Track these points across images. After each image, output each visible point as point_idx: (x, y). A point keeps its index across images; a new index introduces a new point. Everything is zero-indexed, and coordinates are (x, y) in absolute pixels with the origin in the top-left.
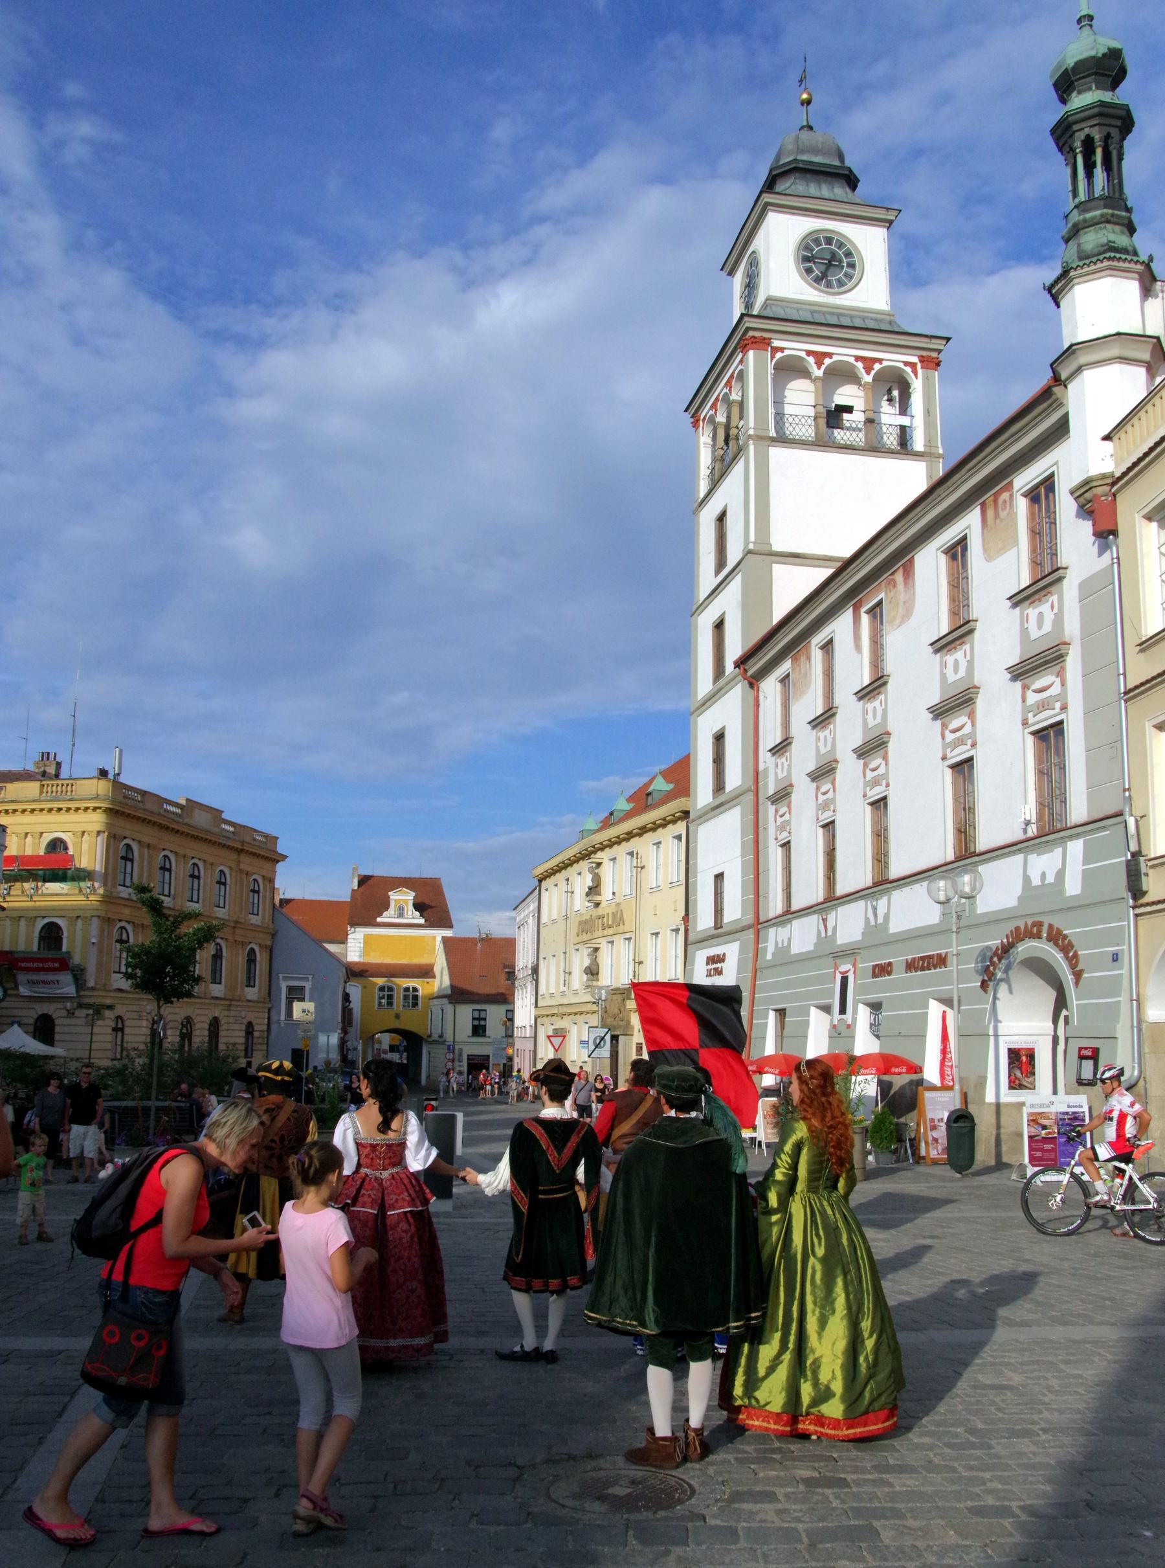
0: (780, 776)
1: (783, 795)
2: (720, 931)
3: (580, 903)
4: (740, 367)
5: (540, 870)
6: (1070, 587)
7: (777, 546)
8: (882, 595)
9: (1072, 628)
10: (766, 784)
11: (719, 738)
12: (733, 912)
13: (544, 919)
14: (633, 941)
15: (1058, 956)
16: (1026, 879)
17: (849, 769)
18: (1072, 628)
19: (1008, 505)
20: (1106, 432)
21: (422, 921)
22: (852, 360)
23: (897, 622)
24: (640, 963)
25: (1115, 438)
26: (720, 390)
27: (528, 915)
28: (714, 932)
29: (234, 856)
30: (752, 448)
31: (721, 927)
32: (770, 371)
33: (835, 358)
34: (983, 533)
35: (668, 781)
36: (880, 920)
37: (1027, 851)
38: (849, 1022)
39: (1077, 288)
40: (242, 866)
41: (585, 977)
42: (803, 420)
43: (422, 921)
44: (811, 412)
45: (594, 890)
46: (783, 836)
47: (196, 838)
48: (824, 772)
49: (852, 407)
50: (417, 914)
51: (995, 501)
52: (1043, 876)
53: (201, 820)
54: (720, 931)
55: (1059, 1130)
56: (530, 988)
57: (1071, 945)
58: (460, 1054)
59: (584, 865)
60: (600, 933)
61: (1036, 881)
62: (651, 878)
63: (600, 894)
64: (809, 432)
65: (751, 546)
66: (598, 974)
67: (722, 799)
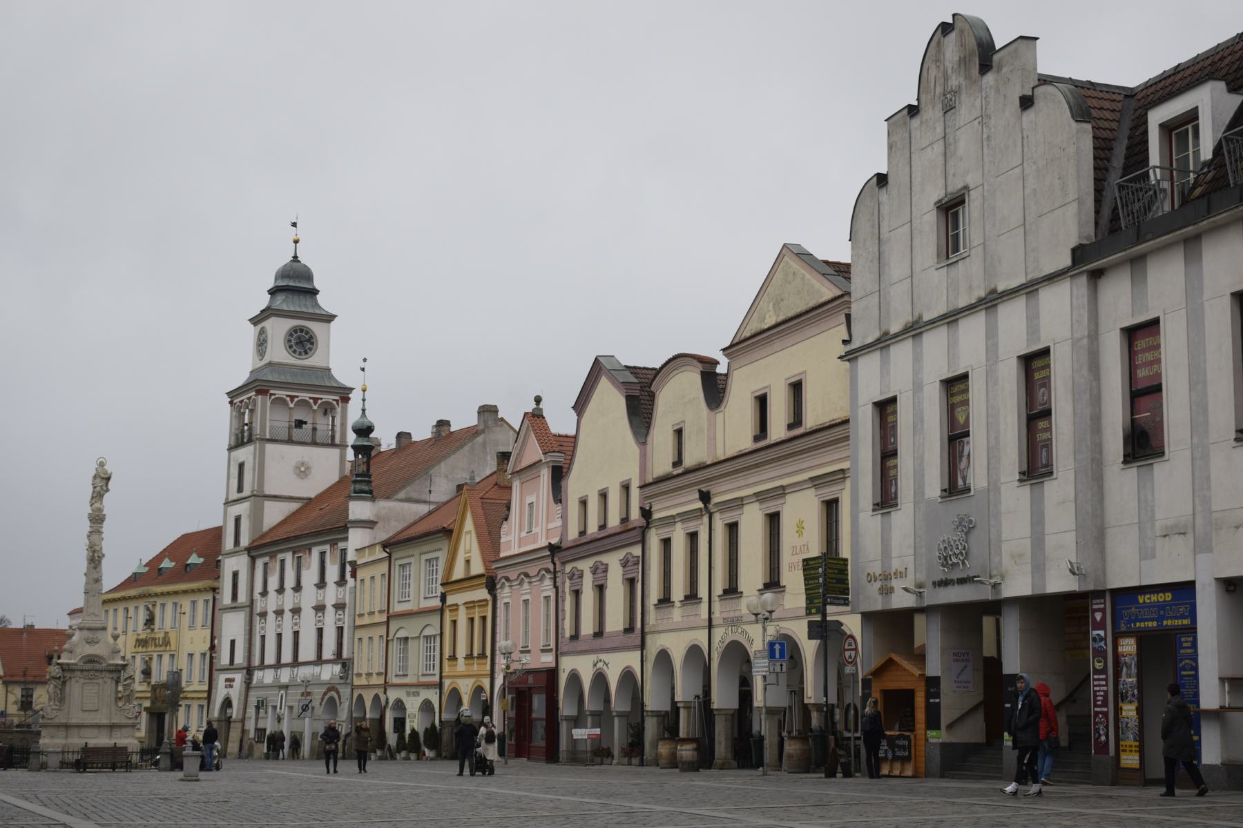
0: (263, 606)
1: (263, 615)
2: (232, 666)
7: (267, 492)
10: (257, 607)
12: (240, 659)
14: (176, 656)
16: (332, 673)
17: (288, 615)
18: (347, 601)
22: (308, 399)
26: (244, 397)
28: (228, 667)
33: (300, 398)
35: (200, 556)
37: (333, 663)
41: (142, 676)
44: (287, 425)
45: (150, 621)
46: (262, 632)
48: (279, 613)
54: (232, 666)
59: (142, 605)
60: (153, 648)
61: (334, 674)
63: (154, 625)
65: (255, 492)
67: (234, 605)
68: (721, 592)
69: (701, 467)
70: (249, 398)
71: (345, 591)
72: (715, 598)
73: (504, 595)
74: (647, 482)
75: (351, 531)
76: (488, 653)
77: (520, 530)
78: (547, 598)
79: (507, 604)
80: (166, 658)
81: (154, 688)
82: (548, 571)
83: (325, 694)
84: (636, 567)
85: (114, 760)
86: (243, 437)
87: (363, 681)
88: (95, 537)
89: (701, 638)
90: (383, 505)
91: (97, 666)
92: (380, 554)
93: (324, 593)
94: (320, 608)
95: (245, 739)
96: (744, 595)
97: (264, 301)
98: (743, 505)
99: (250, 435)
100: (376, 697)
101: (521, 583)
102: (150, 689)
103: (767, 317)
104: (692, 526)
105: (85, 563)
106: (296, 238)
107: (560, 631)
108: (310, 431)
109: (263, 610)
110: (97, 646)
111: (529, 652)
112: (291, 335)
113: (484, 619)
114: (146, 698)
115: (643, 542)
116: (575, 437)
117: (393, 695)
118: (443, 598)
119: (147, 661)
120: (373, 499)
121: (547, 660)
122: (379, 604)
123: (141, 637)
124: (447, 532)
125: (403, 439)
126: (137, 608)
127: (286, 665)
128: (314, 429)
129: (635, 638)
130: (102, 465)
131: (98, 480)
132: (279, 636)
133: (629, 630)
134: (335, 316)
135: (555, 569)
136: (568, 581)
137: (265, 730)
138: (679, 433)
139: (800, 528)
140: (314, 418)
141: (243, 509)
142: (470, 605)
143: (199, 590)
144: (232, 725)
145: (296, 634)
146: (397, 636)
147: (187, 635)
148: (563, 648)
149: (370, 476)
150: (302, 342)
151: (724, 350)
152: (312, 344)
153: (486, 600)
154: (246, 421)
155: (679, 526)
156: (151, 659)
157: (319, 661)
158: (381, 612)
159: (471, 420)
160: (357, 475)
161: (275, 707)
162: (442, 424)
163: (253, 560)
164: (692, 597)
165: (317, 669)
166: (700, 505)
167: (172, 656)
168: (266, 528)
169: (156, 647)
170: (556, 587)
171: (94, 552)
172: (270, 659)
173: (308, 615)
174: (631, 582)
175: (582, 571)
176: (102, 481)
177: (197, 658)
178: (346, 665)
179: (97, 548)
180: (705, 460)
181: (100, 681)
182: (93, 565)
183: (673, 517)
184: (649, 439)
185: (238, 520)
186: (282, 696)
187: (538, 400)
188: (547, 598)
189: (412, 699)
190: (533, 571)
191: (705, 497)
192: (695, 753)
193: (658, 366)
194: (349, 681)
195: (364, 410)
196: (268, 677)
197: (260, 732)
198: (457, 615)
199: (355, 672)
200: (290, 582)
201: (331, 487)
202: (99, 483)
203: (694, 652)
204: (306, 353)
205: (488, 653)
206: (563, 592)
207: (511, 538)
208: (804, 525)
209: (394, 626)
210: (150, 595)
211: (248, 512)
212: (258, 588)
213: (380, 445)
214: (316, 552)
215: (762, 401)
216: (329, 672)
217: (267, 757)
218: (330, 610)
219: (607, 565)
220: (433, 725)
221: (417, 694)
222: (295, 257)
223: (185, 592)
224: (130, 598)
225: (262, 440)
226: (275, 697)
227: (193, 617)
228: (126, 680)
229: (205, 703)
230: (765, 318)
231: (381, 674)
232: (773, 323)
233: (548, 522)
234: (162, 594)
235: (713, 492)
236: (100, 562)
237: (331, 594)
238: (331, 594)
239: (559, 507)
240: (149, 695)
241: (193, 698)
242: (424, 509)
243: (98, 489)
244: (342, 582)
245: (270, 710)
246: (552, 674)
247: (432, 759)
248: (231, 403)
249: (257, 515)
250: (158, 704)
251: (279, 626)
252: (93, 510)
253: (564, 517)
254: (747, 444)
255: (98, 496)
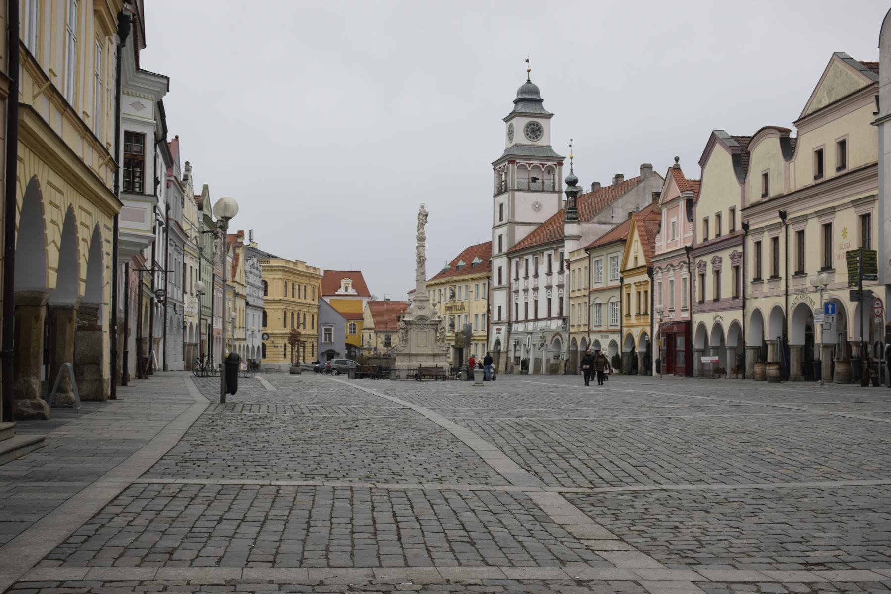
1: (517, 292)
7: (517, 220)
11: (500, 269)
12: (504, 317)
17: (531, 292)
21: (356, 293)
26: (502, 165)
29: (308, 279)
35: (479, 259)
40: (311, 282)
43: (356, 293)
44: (527, 180)
45: (453, 296)
46: (517, 301)
47: (300, 275)
48: (526, 290)
50: (354, 290)
53: (301, 268)
59: (448, 287)
67: (500, 286)
68: (793, 274)
69: (781, 197)
70: (505, 166)
71: (563, 277)
72: (790, 277)
73: (658, 277)
74: (746, 207)
75: (566, 242)
76: (649, 312)
77: (667, 239)
78: (684, 279)
79: (660, 283)
80: (463, 317)
81: (457, 334)
82: (685, 263)
83: (554, 337)
84: (739, 259)
85: (436, 374)
86: (502, 189)
87: (575, 329)
88: (421, 248)
89: (781, 302)
90: (585, 226)
91: (425, 322)
92: (584, 255)
93: (551, 278)
94: (549, 287)
95: (509, 363)
96: (809, 275)
97: (511, 107)
98: (807, 219)
99: (506, 187)
100: (584, 339)
101: (668, 271)
102: (454, 335)
103: (823, 100)
104: (774, 234)
105: (415, 264)
106: (528, 69)
107: (693, 299)
108: (541, 184)
109: (517, 289)
110: (424, 310)
111: (674, 311)
112: (528, 127)
113: (646, 292)
114: (452, 340)
115: (744, 244)
116: (700, 181)
117: (593, 337)
118: (622, 280)
119: (452, 319)
120: (578, 223)
121: (685, 316)
122: (584, 284)
123: (448, 305)
124: (623, 241)
125: (596, 187)
126: (445, 289)
127: (531, 321)
128: (543, 182)
129: (739, 302)
130: (423, 207)
131: (421, 216)
132: (526, 303)
133: (736, 297)
134: (553, 115)
135: (689, 261)
136: (697, 268)
137: (520, 357)
138: (766, 176)
139: (845, 233)
140: (543, 176)
141: (503, 231)
142: (638, 284)
143: (480, 278)
144: (501, 355)
145: (536, 302)
146: (595, 302)
147: (474, 304)
148: (695, 309)
149: (576, 209)
150: (534, 131)
151: (795, 123)
152: (540, 132)
153: (647, 281)
154: (503, 179)
155: (766, 233)
156: (454, 318)
157: (550, 318)
158: (585, 289)
159: (637, 173)
160: (569, 209)
161: (525, 345)
162: (619, 177)
163: (510, 260)
164: (775, 277)
165: (549, 323)
166: (780, 220)
167: (466, 316)
168: (517, 241)
169: (457, 310)
170: (690, 272)
171: (420, 257)
172: (521, 317)
173: (542, 291)
174: (737, 268)
175: (706, 262)
176: (424, 216)
177: (480, 317)
178: (565, 320)
179: (422, 255)
180: (783, 192)
181: (427, 330)
182: (420, 265)
183: (762, 228)
184: (747, 181)
185: (500, 237)
187: (677, 159)
188: (684, 279)
189: (604, 339)
190: (675, 263)
191: (783, 215)
192: (778, 371)
193: (752, 135)
194: (567, 329)
195: (572, 170)
196: (520, 327)
197: (517, 359)
198: (630, 290)
199: (571, 324)
200: (531, 272)
201: (553, 217)
202: (422, 218)
203: (776, 310)
204: (537, 137)
205: (649, 312)
206: (694, 275)
207: (662, 243)
208: (847, 230)
209: (592, 297)
210: (453, 282)
211: (506, 232)
212: (513, 276)
213: (582, 191)
214: (546, 254)
215: (820, 154)
216: (556, 324)
217: (521, 373)
218: (555, 289)
219: (721, 258)
220: (617, 355)
221: (607, 337)
222: (529, 80)
223: (472, 279)
224: (442, 283)
225: (513, 190)
226: (525, 339)
227: (477, 294)
228: (441, 329)
229: (485, 342)
230: (821, 102)
231: (586, 325)
232: (827, 104)
233: (684, 234)
234: (459, 281)
235: (787, 212)
236: (424, 263)
237: (556, 279)
238: (556, 279)
239: (691, 224)
240: (454, 338)
241: (479, 340)
242: (609, 228)
243: (421, 221)
244: (561, 271)
245: (522, 346)
246: (688, 324)
247: (617, 375)
248: (494, 169)
249: (511, 234)
250: (459, 343)
251: (526, 298)
252: (419, 234)
253: (694, 230)
254: (810, 181)
255: (421, 225)
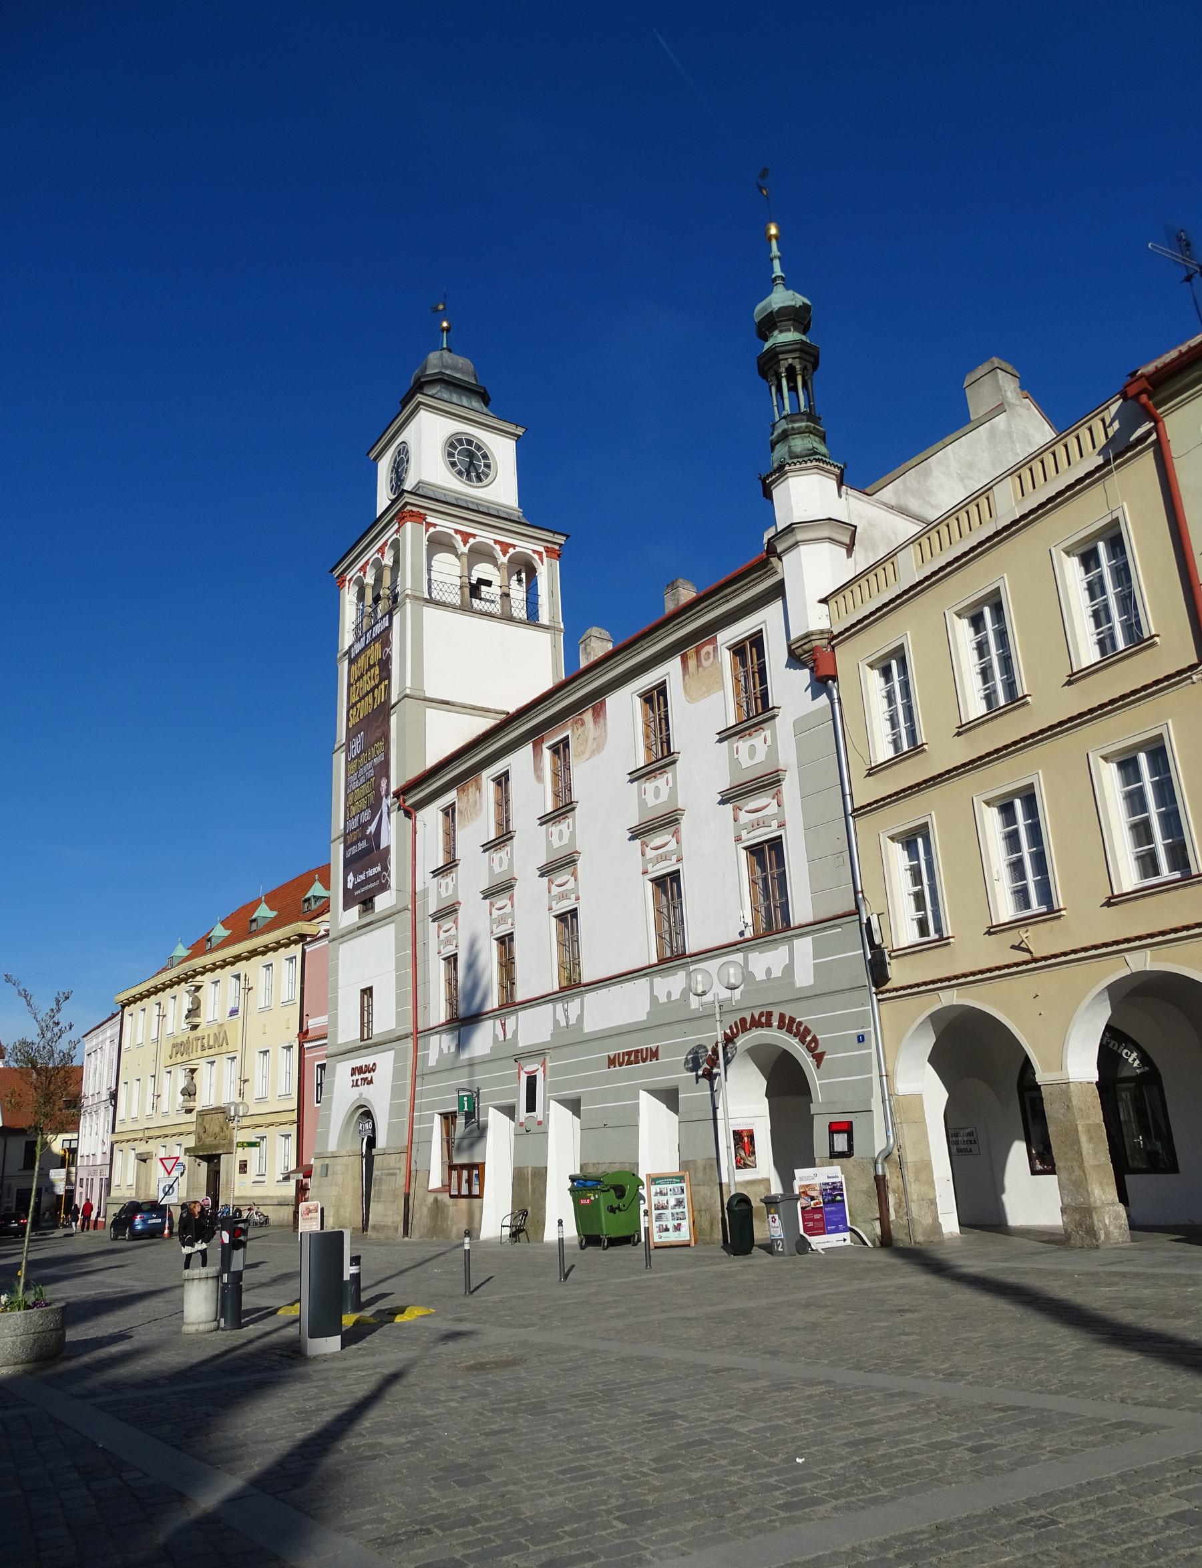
2: (367, 1042)
3: (176, 1024)
4: (395, 536)
5: (124, 996)
6: (783, 725)
7: (428, 695)
8: (568, 732)
9: (788, 757)
10: (425, 904)
13: (125, 1045)
15: (793, 1042)
18: (788, 757)
19: (712, 656)
20: (823, 597)
22: (491, 543)
23: (587, 755)
24: (245, 1081)
25: (832, 602)
27: (103, 1041)
30: (408, 606)
31: (369, 1038)
32: (425, 542)
33: (478, 539)
34: (684, 680)
35: (272, 909)
36: (572, 1021)
38: (540, 1118)
39: (790, 480)
41: (180, 1098)
42: (451, 587)
44: (458, 582)
45: (193, 1012)
48: (500, 889)
49: (491, 582)
51: (698, 653)
52: (769, 971)
54: (367, 1042)
55: (823, 1200)
56: (104, 1116)
57: (807, 1031)
58: (9, 1189)
60: (200, 1053)
62: (259, 997)
64: (457, 600)
65: (408, 691)
66: (195, 1094)
168: (431, 761)
186: (532, 1082)
240: (193, 1128)
